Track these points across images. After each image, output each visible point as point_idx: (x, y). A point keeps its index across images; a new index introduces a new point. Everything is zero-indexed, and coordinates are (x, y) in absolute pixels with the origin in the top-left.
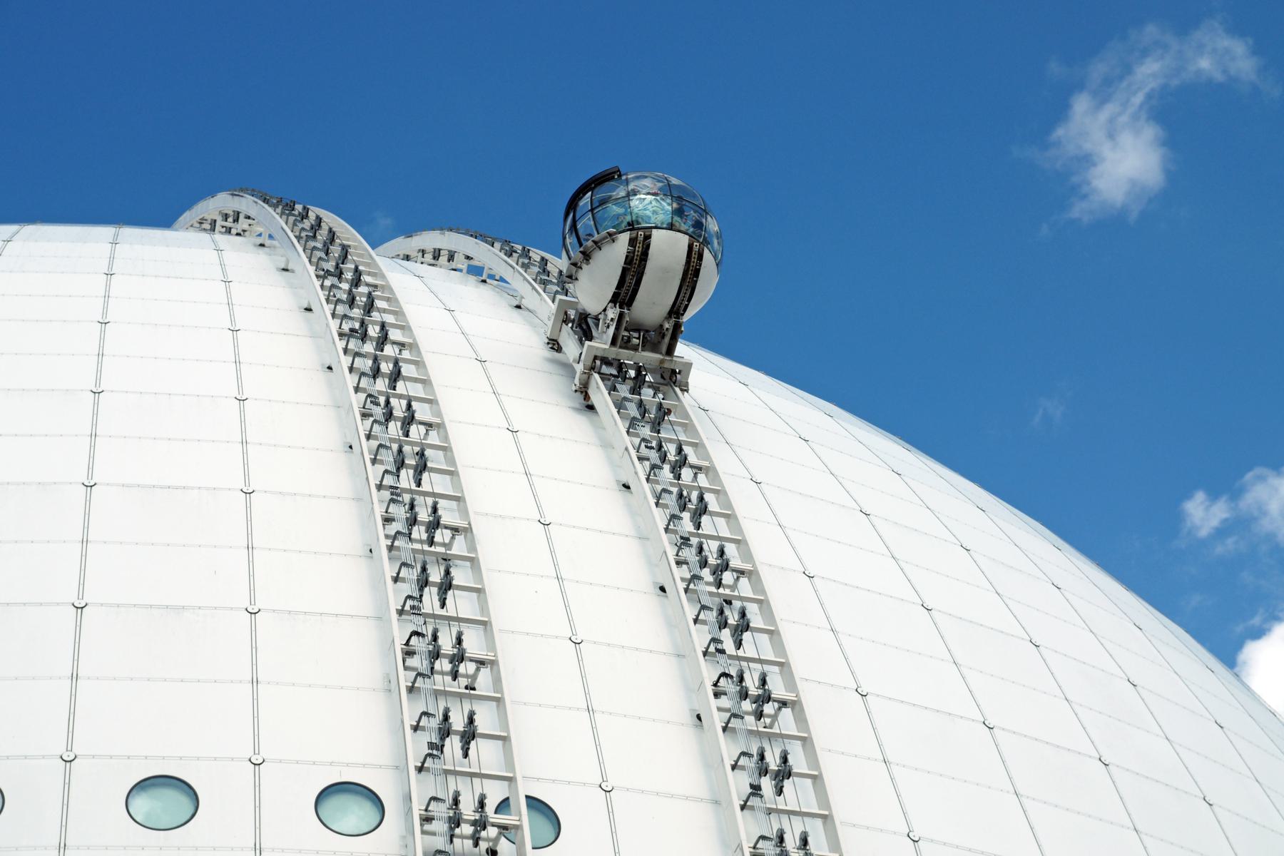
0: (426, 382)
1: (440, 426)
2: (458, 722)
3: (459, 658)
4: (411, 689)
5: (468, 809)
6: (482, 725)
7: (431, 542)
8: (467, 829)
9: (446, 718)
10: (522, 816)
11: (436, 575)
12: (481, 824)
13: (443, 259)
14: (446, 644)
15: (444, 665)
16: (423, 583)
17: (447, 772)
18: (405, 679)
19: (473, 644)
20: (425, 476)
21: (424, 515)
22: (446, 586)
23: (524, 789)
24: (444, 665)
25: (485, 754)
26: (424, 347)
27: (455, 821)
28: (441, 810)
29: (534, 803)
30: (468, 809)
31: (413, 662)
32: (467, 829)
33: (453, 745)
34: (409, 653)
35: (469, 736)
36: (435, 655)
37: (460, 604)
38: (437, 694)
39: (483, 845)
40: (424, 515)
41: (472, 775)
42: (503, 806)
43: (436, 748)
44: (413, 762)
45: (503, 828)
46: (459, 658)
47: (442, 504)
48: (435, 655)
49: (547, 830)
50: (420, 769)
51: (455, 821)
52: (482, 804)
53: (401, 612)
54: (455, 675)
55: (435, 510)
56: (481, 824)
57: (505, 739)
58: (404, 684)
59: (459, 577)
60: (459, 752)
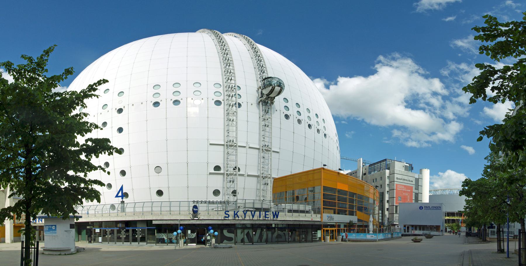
0: (228, 47)
1: (230, 51)
2: (230, 78)
3: (231, 72)
4: (225, 75)
5: (231, 86)
6: (233, 78)
7: (228, 61)
8: (230, 88)
9: (229, 78)
10: (236, 87)
11: (228, 65)
12: (232, 88)
13: (231, 35)
14: (229, 71)
15: (229, 73)
16: (227, 65)
17: (228, 83)
18: (224, 74)
19: (232, 71)
20: (228, 55)
21: (227, 59)
22: (230, 66)
23: (237, 85)
24: (229, 73)
25: (233, 82)
26: (228, 43)
27: (229, 87)
28: (228, 86)
29: (238, 86)
30: (231, 86)
31: (225, 73)
32: (230, 88)
33: (229, 81)
34: (225, 72)
35: (231, 80)
36: (228, 72)
37: (231, 67)
38: (228, 76)
39: (232, 90)
40: (227, 59)
41: (231, 83)
42: (235, 86)
43: (228, 81)
44: (225, 82)
45: (234, 88)
46: (231, 72)
47: (229, 58)
48: (228, 72)
49: (239, 89)
50: (225, 82)
51: (229, 87)
52: (232, 86)
53: (224, 68)
54: (230, 74)
55: (229, 58)
56: (232, 88)
57: (235, 80)
58: (224, 74)
59: (231, 65)
60: (230, 81)
